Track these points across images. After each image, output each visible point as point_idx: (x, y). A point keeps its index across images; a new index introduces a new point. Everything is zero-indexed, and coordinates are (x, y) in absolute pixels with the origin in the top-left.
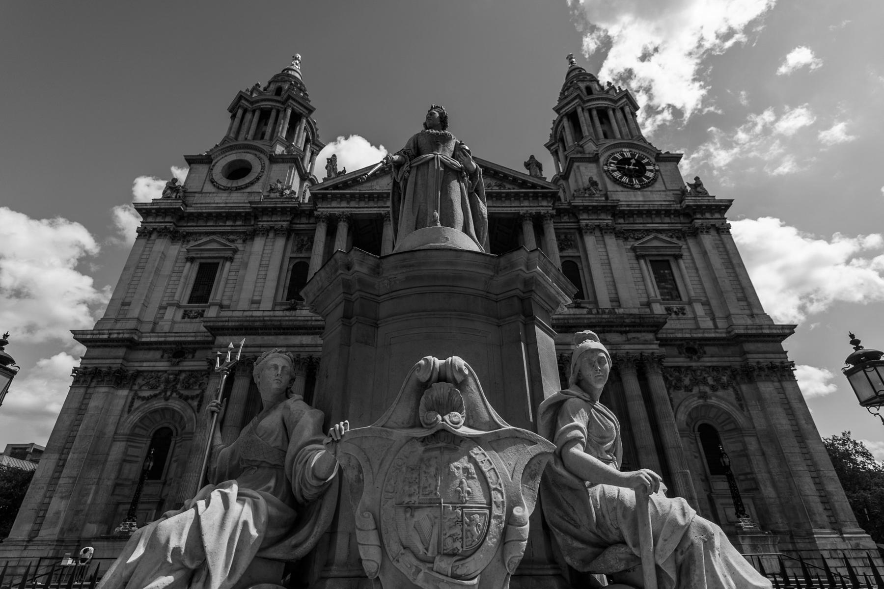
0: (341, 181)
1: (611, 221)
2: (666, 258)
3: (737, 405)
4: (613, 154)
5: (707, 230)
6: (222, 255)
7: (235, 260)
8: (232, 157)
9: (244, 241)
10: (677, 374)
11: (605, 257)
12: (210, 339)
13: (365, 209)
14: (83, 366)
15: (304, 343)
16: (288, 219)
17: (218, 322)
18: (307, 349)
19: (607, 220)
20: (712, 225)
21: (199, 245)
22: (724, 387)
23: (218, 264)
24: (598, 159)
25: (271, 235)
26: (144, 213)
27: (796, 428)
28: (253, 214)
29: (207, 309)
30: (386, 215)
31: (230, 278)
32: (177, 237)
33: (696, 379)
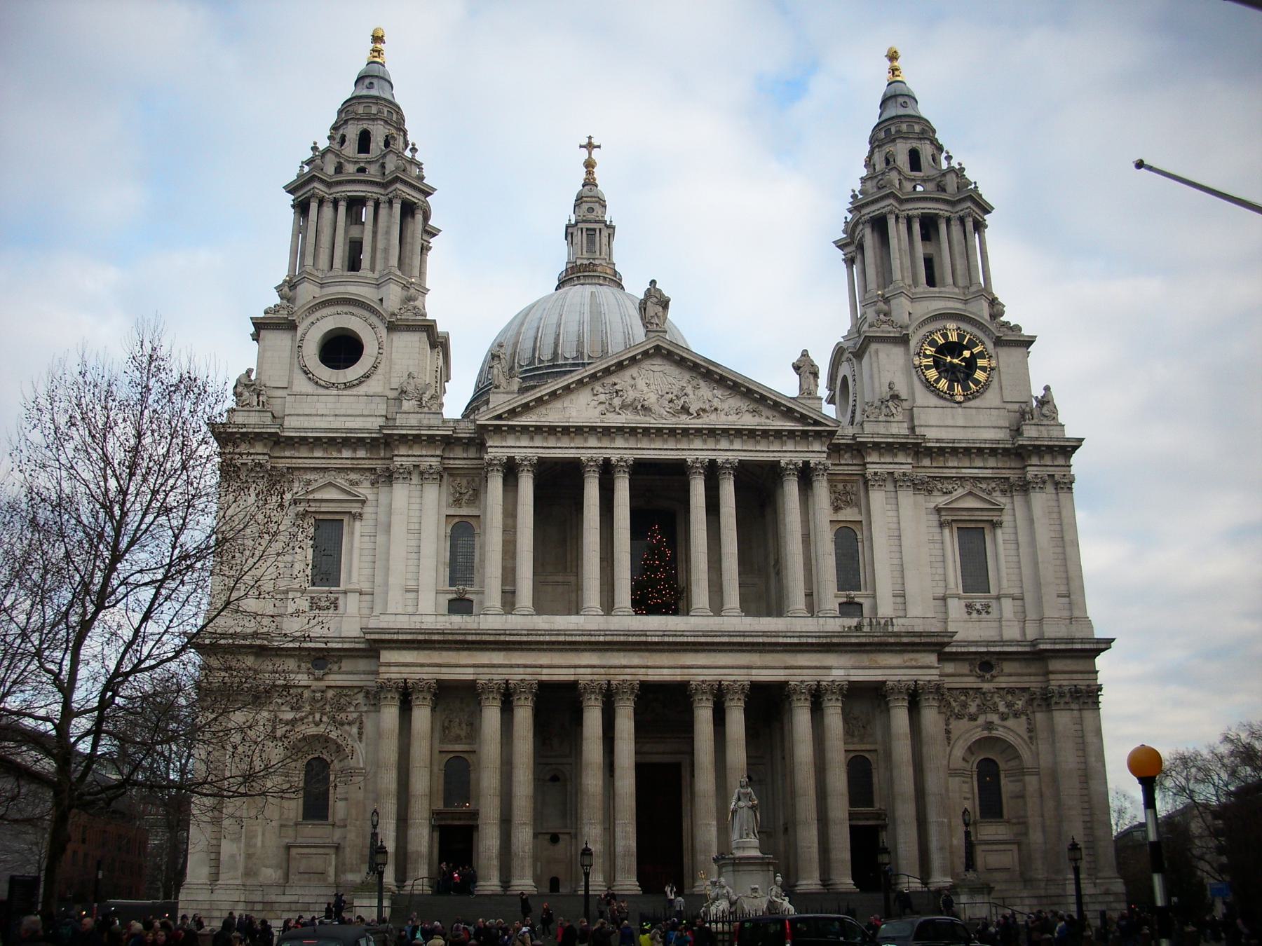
0: (520, 403)
1: (910, 466)
3: (1026, 738)
4: (931, 333)
6: (347, 510)
7: (365, 516)
9: (373, 484)
10: (963, 698)
11: (895, 526)
12: (362, 646)
15: (495, 662)
16: (438, 452)
18: (500, 670)
19: (903, 464)
20: (1049, 475)
22: (1016, 715)
27: (1083, 766)
29: (341, 597)
33: (984, 705)
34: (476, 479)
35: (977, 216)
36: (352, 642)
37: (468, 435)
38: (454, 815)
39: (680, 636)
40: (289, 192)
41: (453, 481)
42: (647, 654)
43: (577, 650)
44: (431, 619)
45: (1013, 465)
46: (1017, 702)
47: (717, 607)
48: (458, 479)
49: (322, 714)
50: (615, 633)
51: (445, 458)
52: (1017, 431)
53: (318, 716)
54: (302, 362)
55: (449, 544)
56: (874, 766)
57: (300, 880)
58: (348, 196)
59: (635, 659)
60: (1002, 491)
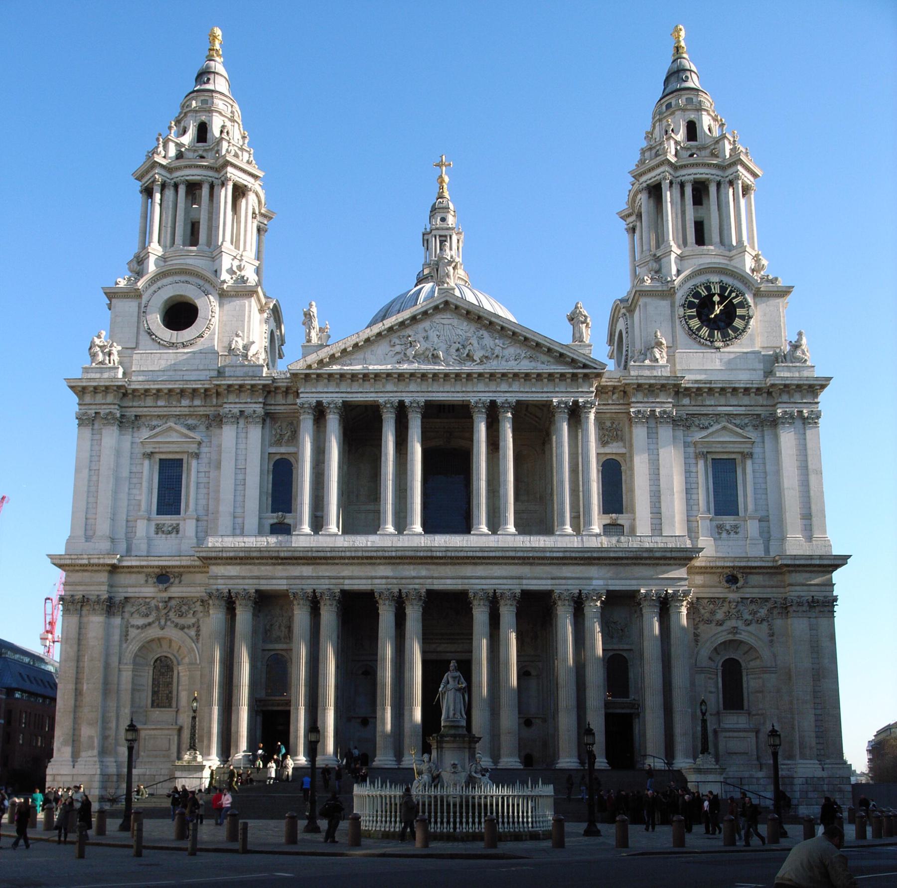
1: (671, 405)
2: (733, 456)
4: (696, 286)
5: (790, 419)
8: (171, 290)
9: (207, 428)
10: (712, 606)
12: (198, 563)
13: (359, 395)
14: (68, 593)
16: (261, 400)
18: (309, 581)
21: (155, 436)
24: (675, 293)
25: (242, 421)
28: (215, 391)
31: (201, 480)
34: (295, 422)
35: (745, 179)
37: (285, 384)
39: (461, 551)
40: (139, 179)
42: (434, 567)
43: (374, 564)
44: (253, 539)
45: (765, 403)
46: (760, 610)
47: (495, 525)
48: (279, 424)
51: (267, 405)
52: (771, 372)
55: (271, 477)
56: (630, 663)
58: (187, 180)
59: (423, 571)
60: (754, 426)
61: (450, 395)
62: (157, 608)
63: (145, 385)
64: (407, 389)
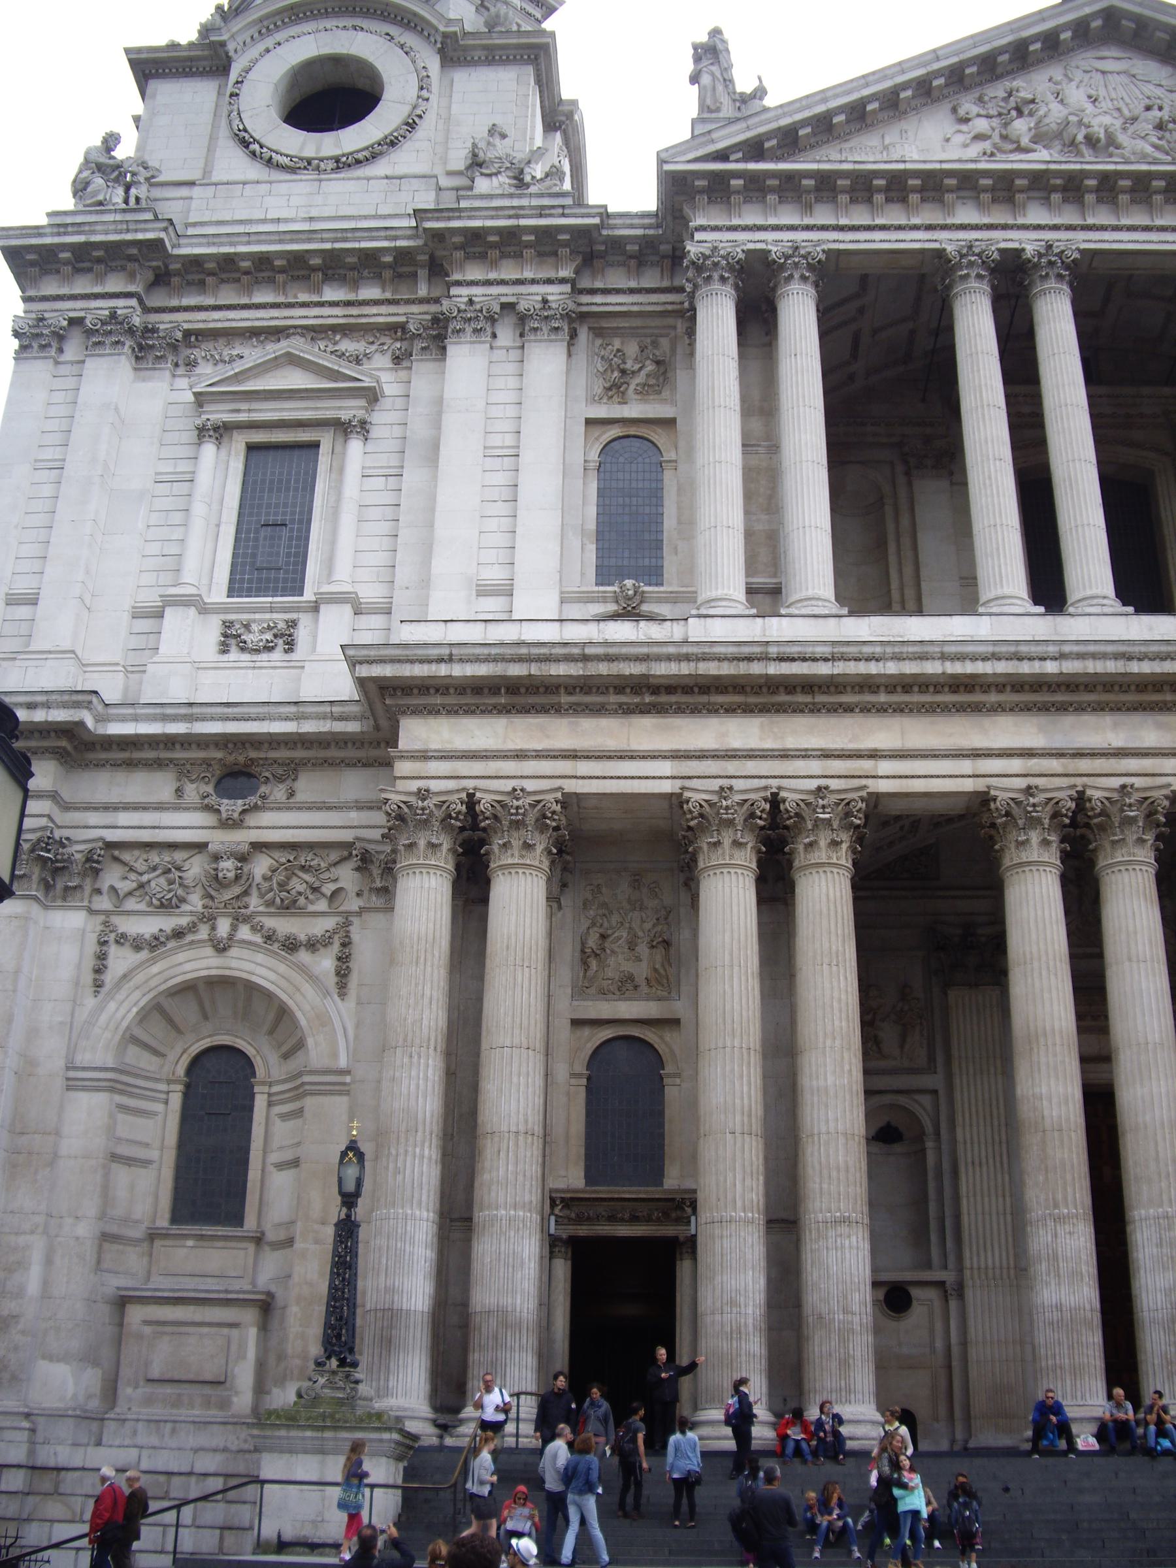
0: (774, 125)
6: (330, 414)
7: (375, 432)
9: (397, 360)
12: (352, 727)
16: (564, 273)
17: (412, 662)
18: (752, 767)
21: (237, 377)
23: (315, 445)
25: (506, 334)
26: (32, 264)
28: (424, 258)
29: (304, 620)
30: (962, 256)
32: (152, 347)
34: (665, 343)
36: (323, 717)
37: (640, 232)
38: (615, 1210)
41: (604, 346)
43: (977, 709)
48: (617, 343)
49: (238, 920)
50: (1092, 648)
51: (581, 292)
53: (223, 927)
54: (237, 122)
55: (593, 486)
57: (149, 1401)
61: (1154, 236)
62: (218, 881)
63: (222, 244)
64: (1020, 221)
